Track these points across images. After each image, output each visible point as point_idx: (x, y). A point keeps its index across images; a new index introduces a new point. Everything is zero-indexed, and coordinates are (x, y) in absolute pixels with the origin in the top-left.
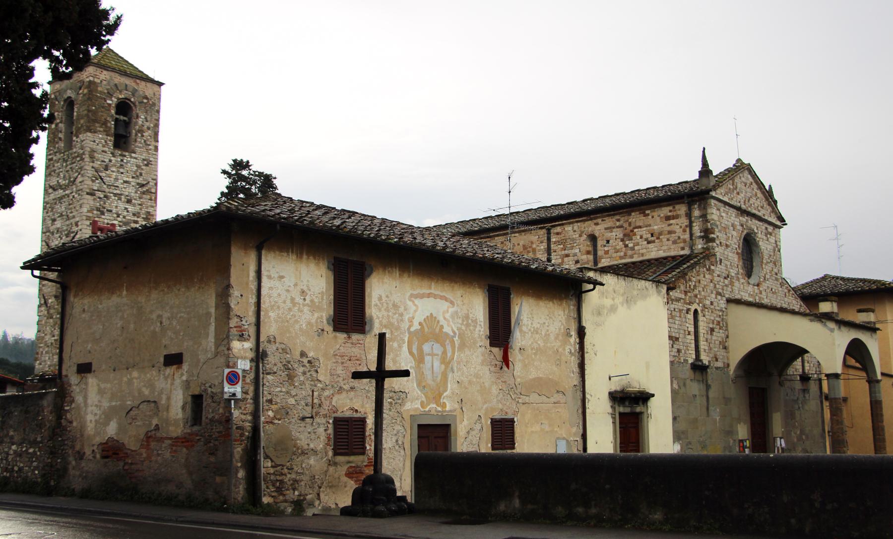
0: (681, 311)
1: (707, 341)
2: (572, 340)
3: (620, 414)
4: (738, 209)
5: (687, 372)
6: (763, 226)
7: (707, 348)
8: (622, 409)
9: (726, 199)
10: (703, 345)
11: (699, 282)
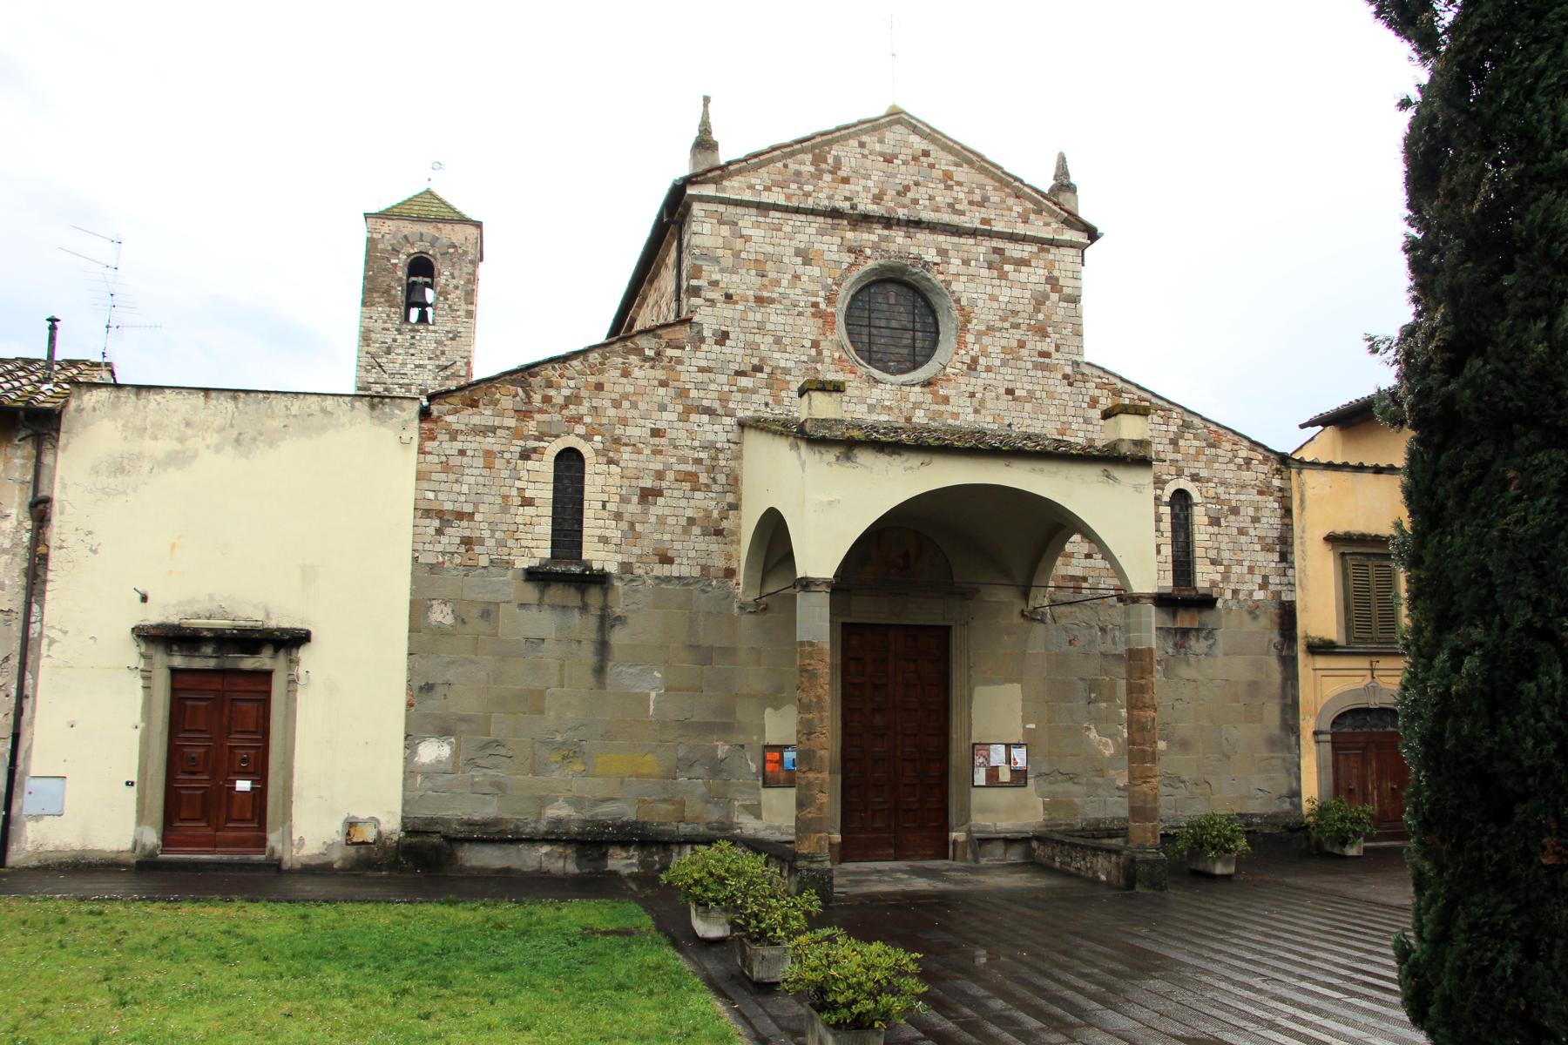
0: (489, 454)
1: (618, 516)
2: (8, 525)
3: (174, 671)
4: (835, 213)
5: (512, 588)
6: (982, 248)
7: (615, 535)
8: (179, 661)
9: (776, 197)
10: (593, 524)
11: (599, 387)
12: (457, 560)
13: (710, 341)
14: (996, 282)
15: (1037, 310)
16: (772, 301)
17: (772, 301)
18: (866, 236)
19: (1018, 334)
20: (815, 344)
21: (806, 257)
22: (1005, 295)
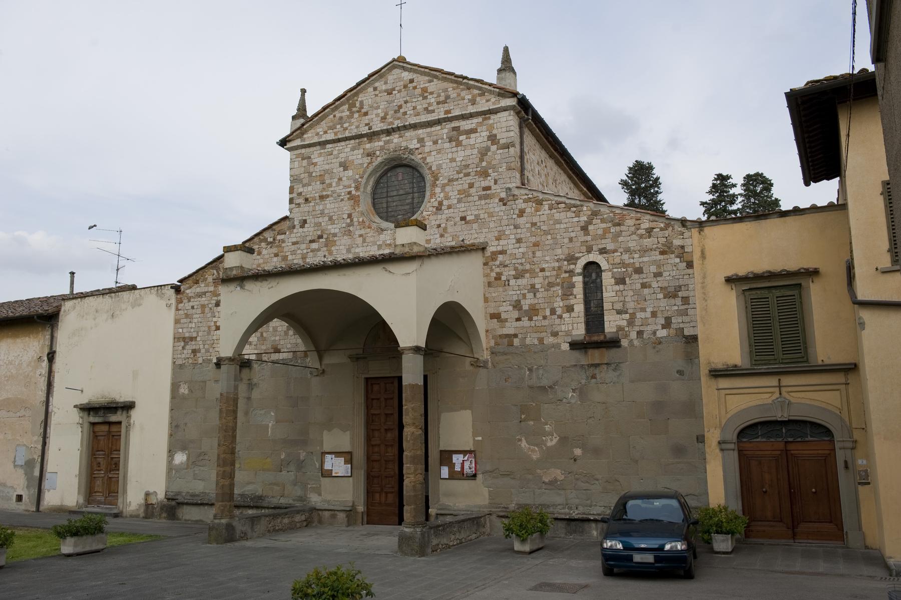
12: (190, 361)
13: (298, 227)
14: (454, 149)
15: (481, 160)
16: (327, 196)
17: (327, 196)
18: (377, 144)
19: (468, 180)
20: (350, 216)
21: (345, 166)
22: (460, 155)
